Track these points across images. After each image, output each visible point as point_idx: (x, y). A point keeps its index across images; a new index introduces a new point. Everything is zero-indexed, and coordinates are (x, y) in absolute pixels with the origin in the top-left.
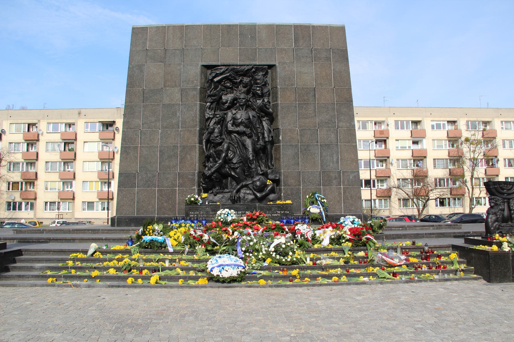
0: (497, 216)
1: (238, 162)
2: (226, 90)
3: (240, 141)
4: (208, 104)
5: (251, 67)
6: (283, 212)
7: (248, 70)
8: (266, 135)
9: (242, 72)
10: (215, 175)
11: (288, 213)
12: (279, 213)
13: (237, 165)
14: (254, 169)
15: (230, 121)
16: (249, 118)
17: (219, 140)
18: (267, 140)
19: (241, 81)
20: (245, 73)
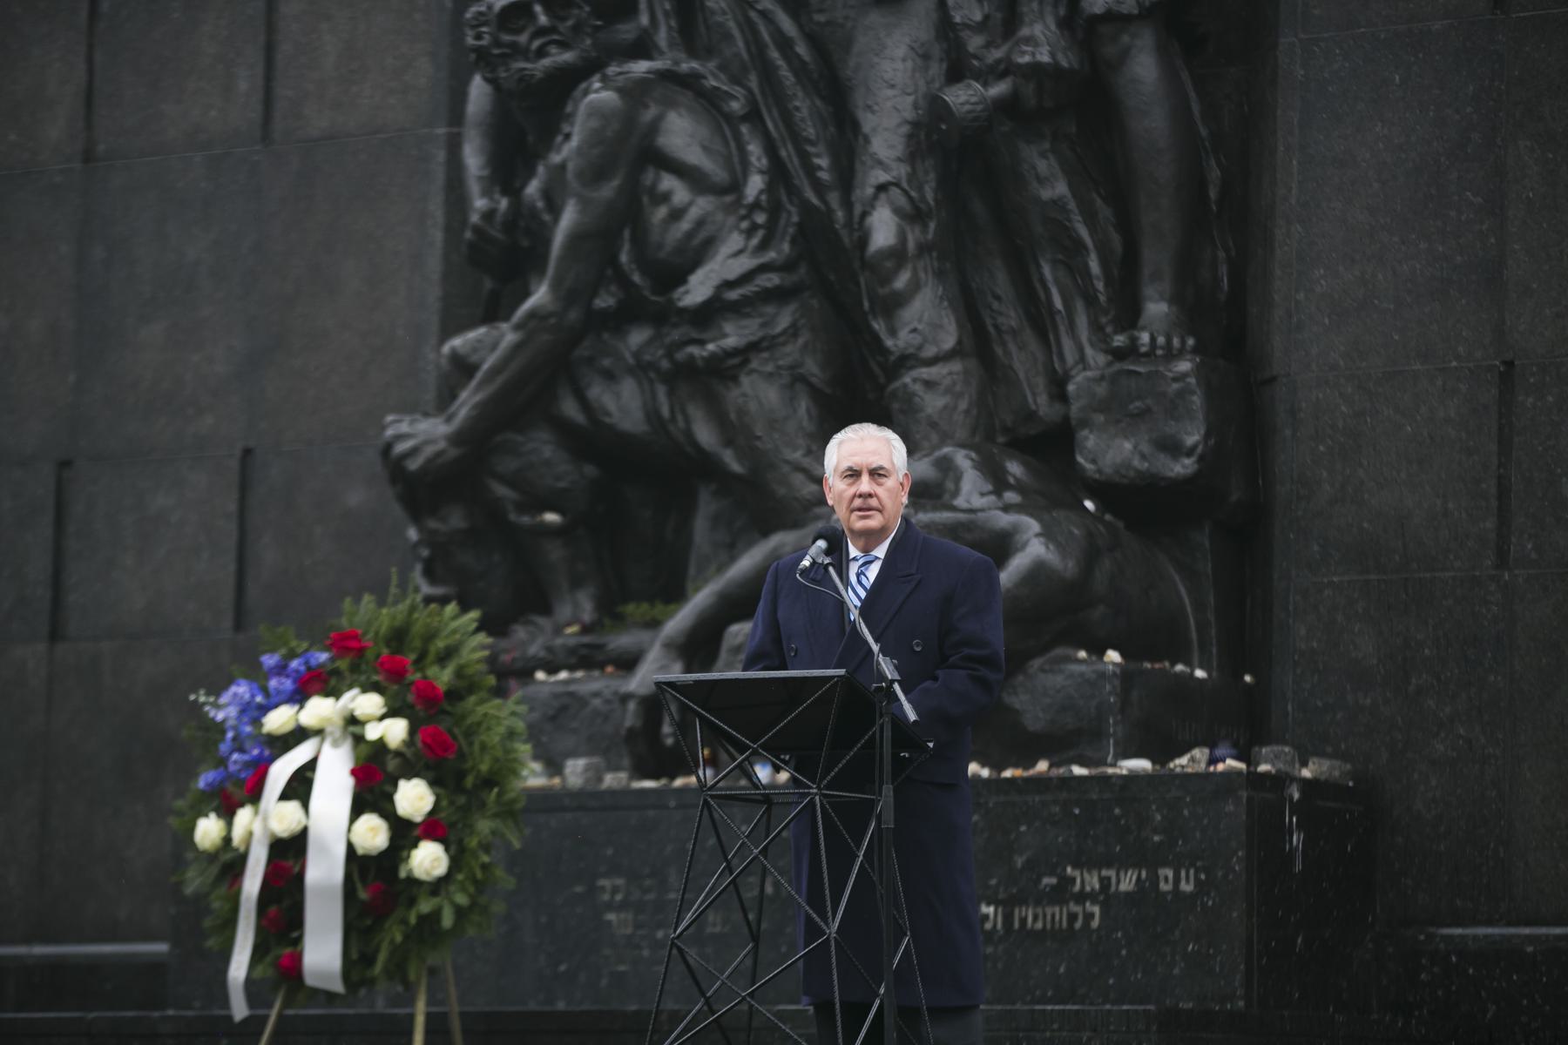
1: (733, 295)
3: (785, 45)
6: (1127, 882)
11: (1187, 887)
12: (1092, 896)
13: (733, 335)
14: (907, 379)
17: (541, 53)
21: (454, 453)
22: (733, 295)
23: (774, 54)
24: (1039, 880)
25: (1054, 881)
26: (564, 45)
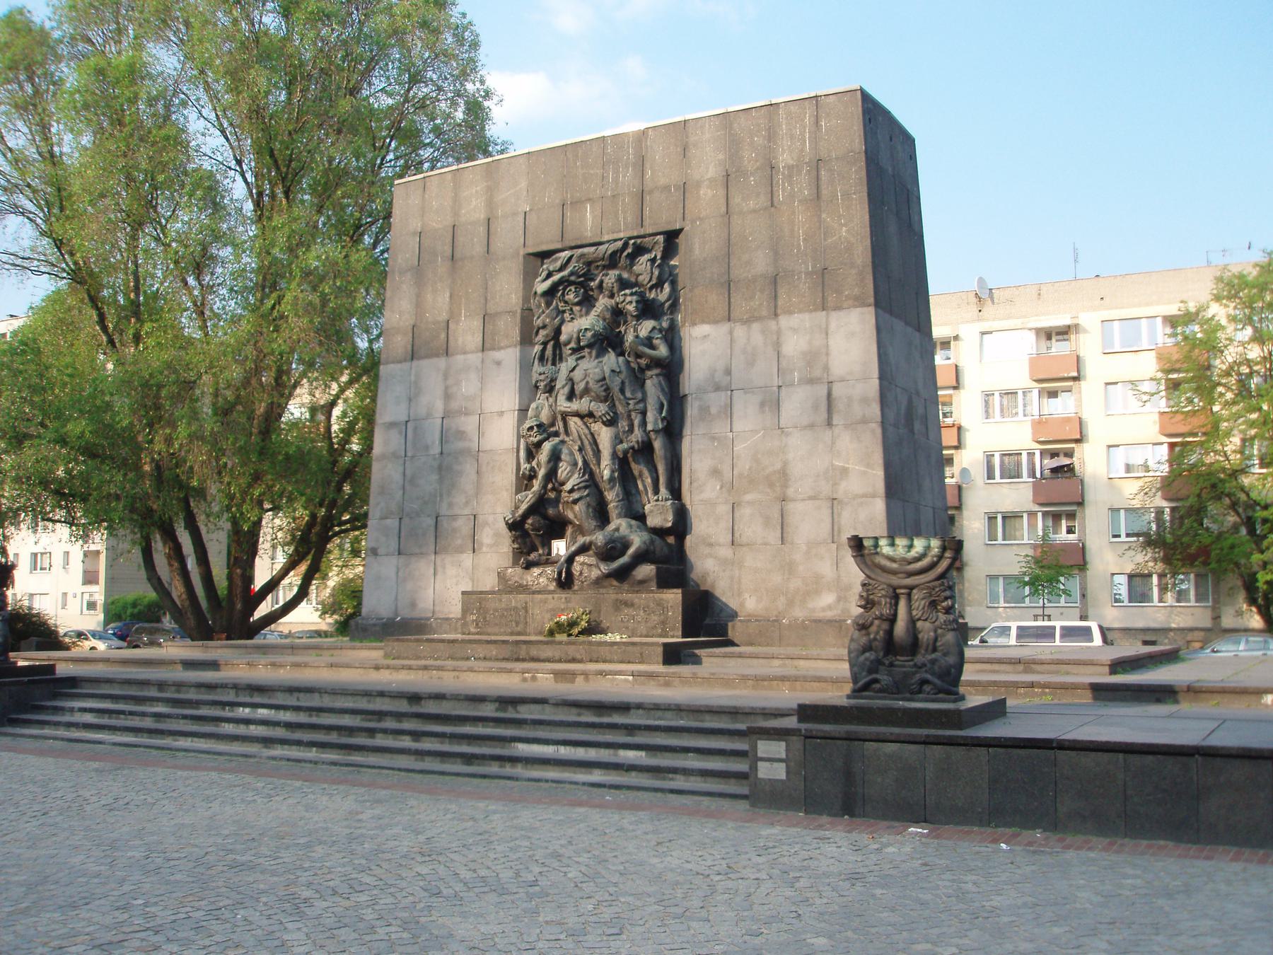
0: (868, 634)
2: (571, 310)
4: (537, 348)
5: (620, 244)
7: (614, 253)
8: (651, 416)
9: (603, 259)
10: (530, 521)
15: (563, 387)
16: (604, 379)
18: (650, 427)
19: (602, 282)
20: (612, 261)
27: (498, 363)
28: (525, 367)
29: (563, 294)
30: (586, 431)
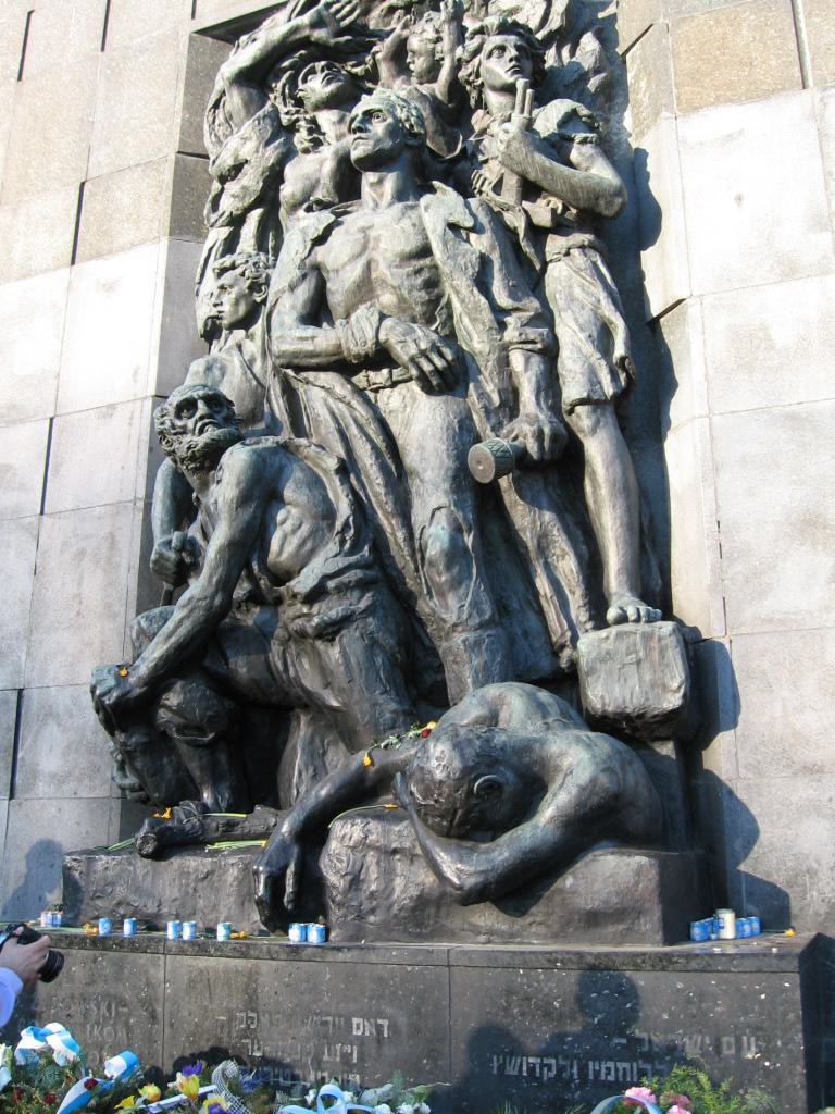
10: (173, 699)
15: (292, 288)
16: (425, 251)
17: (202, 431)
21: (138, 691)
22: (331, 584)
23: (354, 431)
24: (610, 1039)
25: (624, 1041)
26: (218, 426)
27: (109, 287)
28: (178, 290)
29: (293, 82)
30: (362, 411)
